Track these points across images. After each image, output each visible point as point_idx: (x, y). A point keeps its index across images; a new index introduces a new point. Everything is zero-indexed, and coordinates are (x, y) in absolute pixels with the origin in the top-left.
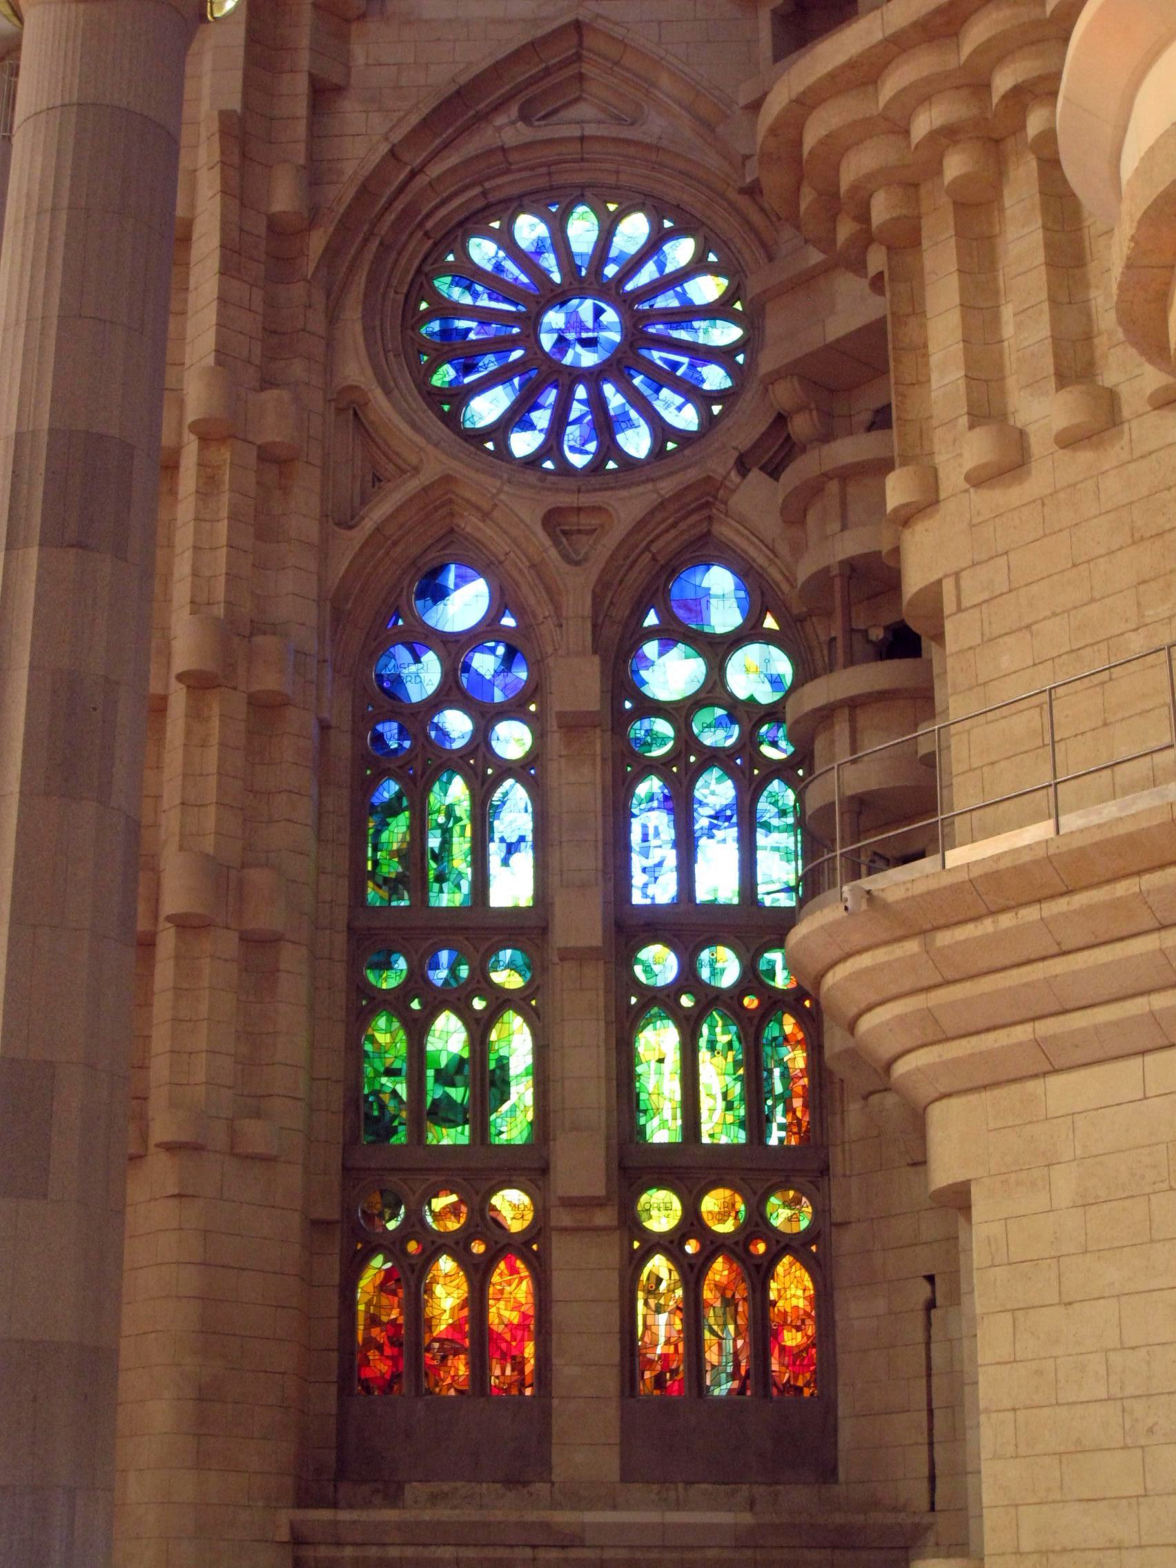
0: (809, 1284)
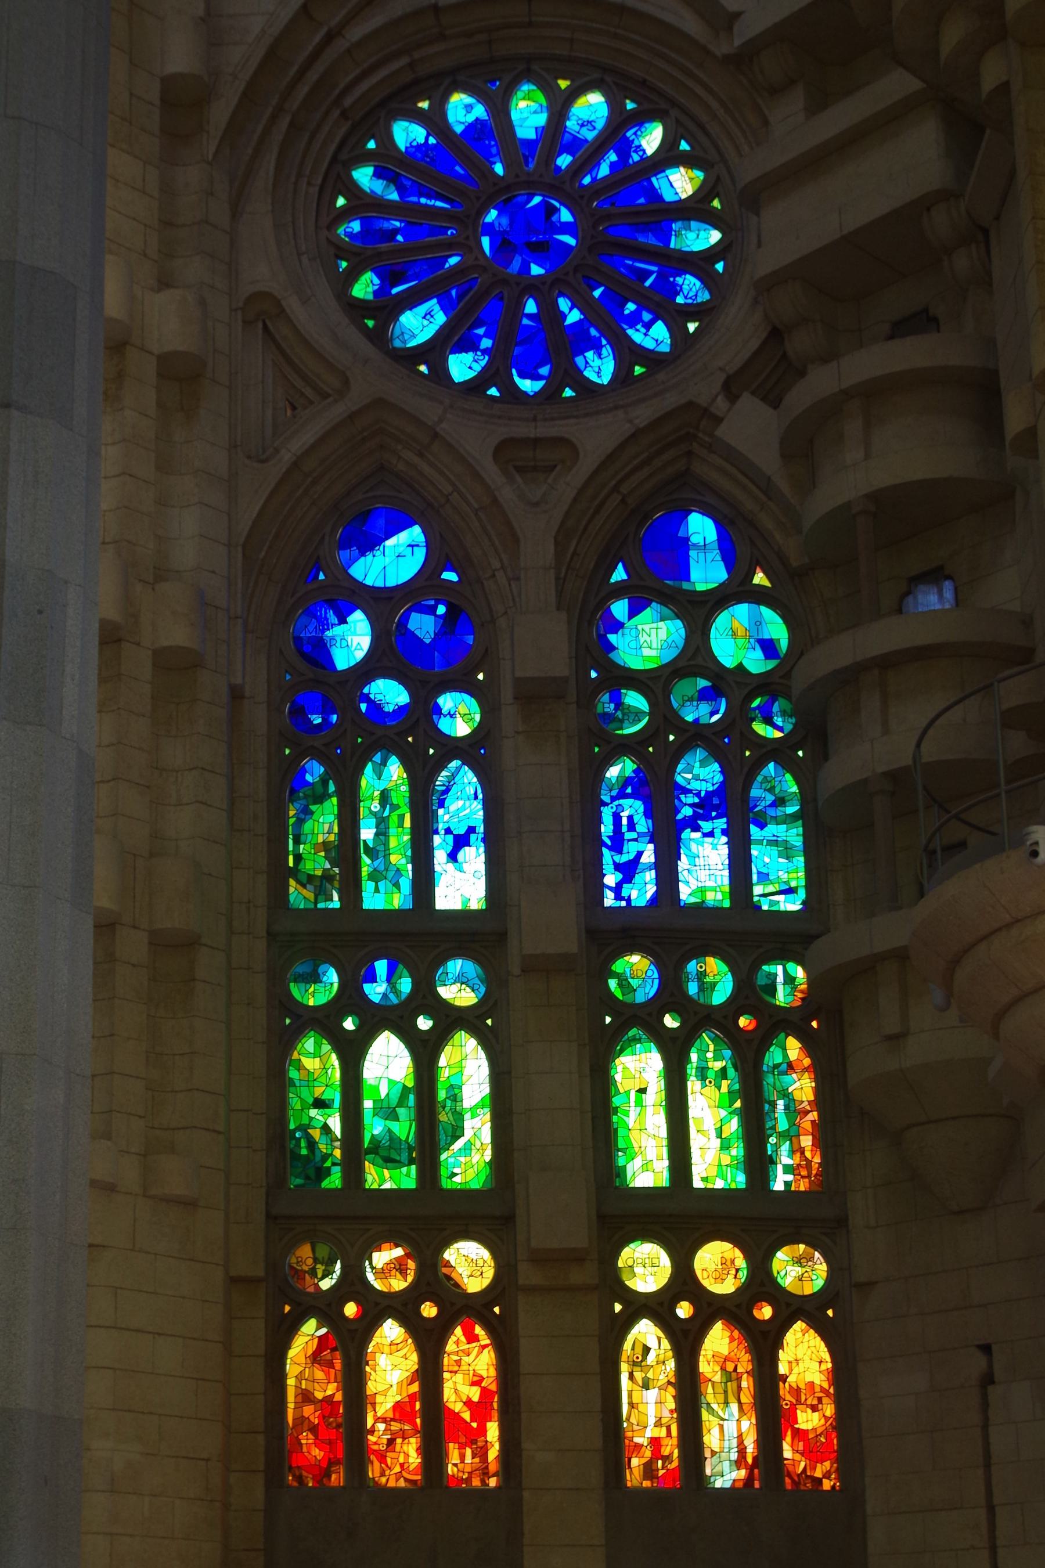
0: (827, 1357)
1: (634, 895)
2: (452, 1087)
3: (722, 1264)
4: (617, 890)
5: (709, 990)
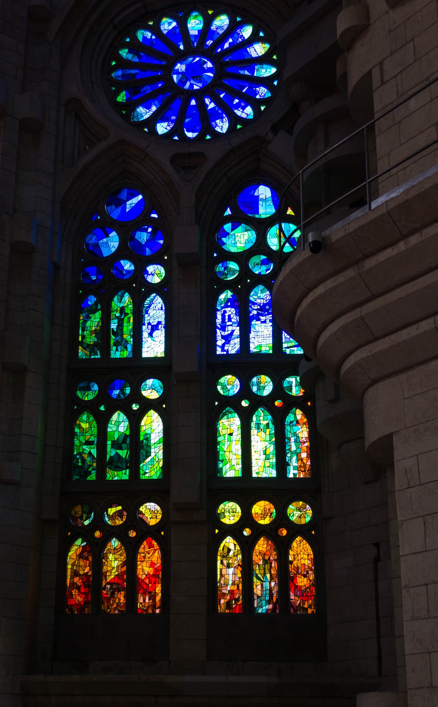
0: (311, 552)
2: (146, 434)
3: (264, 511)
4: (223, 347)
5: (262, 390)
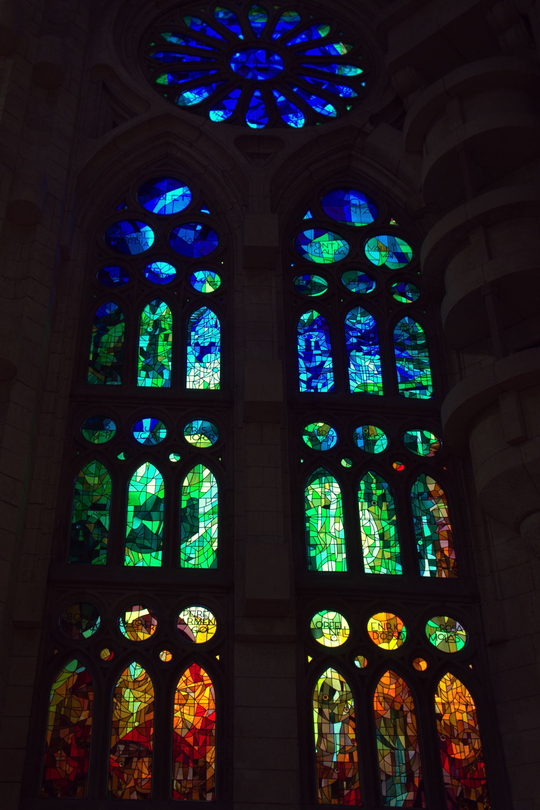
1: (320, 386)
2: (192, 499)
3: (387, 629)
4: (308, 382)
5: (371, 445)
